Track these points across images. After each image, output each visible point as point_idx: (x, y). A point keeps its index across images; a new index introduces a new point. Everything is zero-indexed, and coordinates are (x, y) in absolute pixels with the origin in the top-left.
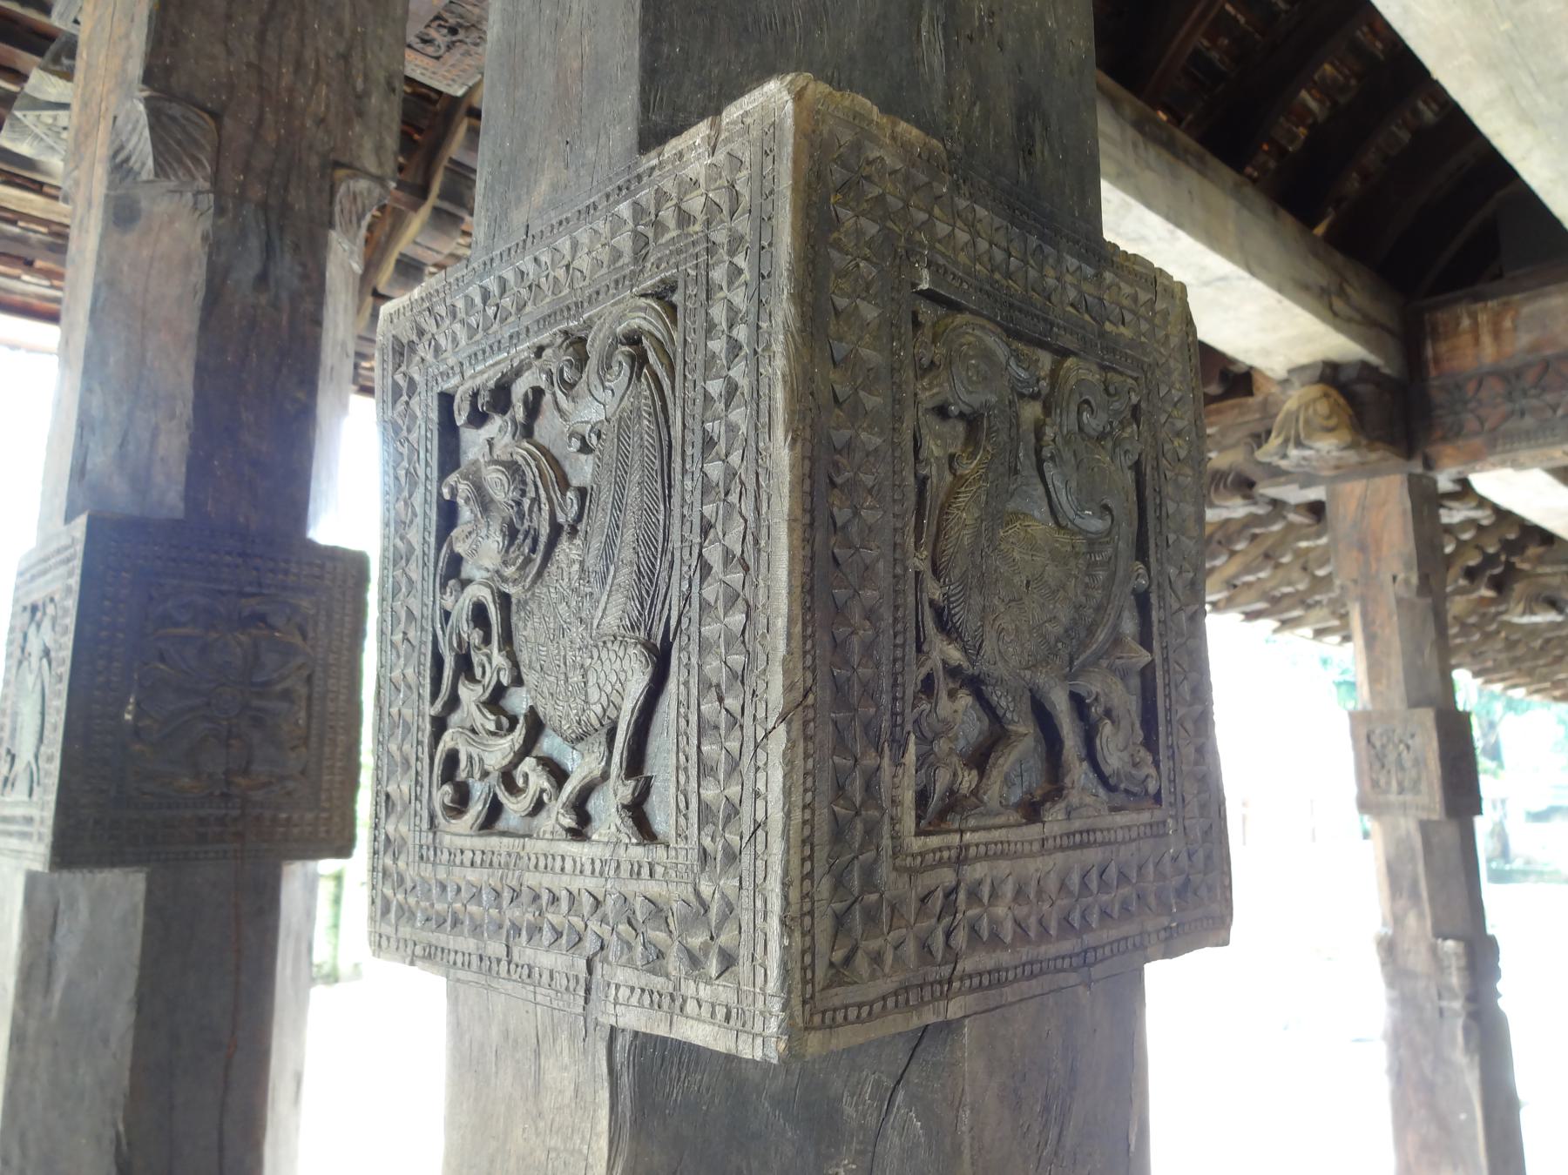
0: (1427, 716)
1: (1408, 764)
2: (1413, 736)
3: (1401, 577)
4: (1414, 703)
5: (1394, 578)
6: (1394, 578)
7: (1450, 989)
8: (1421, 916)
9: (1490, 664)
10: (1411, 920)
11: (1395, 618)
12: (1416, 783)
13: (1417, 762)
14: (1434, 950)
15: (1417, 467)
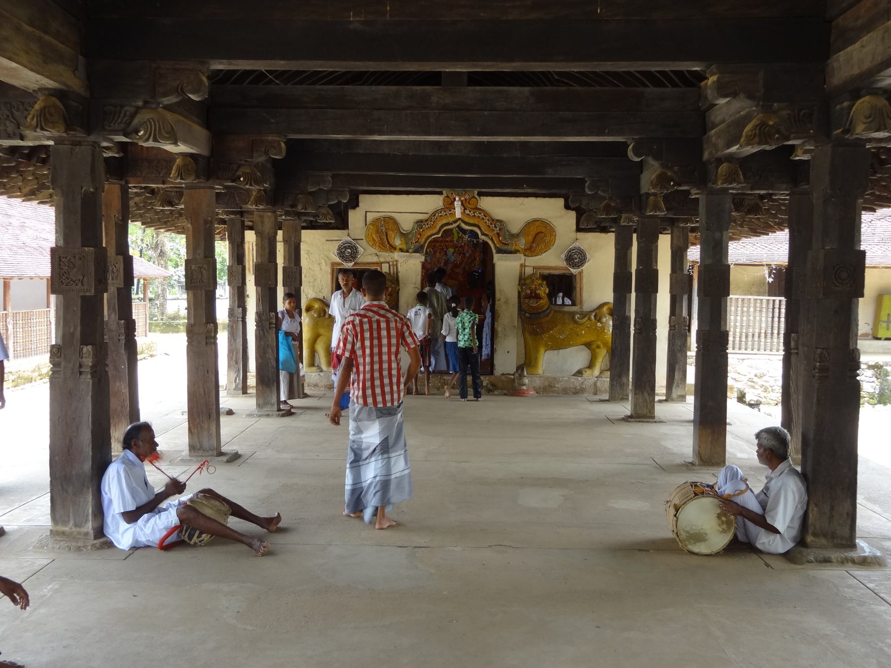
0: (121, 258)
1: (115, 271)
2: (117, 263)
3: (117, 216)
4: (117, 254)
5: (115, 216)
6: (115, 216)
7: (122, 333)
8: (116, 314)
9: (149, 220)
10: (113, 316)
11: (114, 228)
12: (117, 277)
13: (117, 271)
14: (118, 324)
15: (123, 183)
